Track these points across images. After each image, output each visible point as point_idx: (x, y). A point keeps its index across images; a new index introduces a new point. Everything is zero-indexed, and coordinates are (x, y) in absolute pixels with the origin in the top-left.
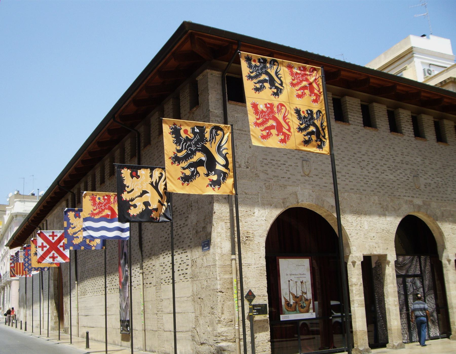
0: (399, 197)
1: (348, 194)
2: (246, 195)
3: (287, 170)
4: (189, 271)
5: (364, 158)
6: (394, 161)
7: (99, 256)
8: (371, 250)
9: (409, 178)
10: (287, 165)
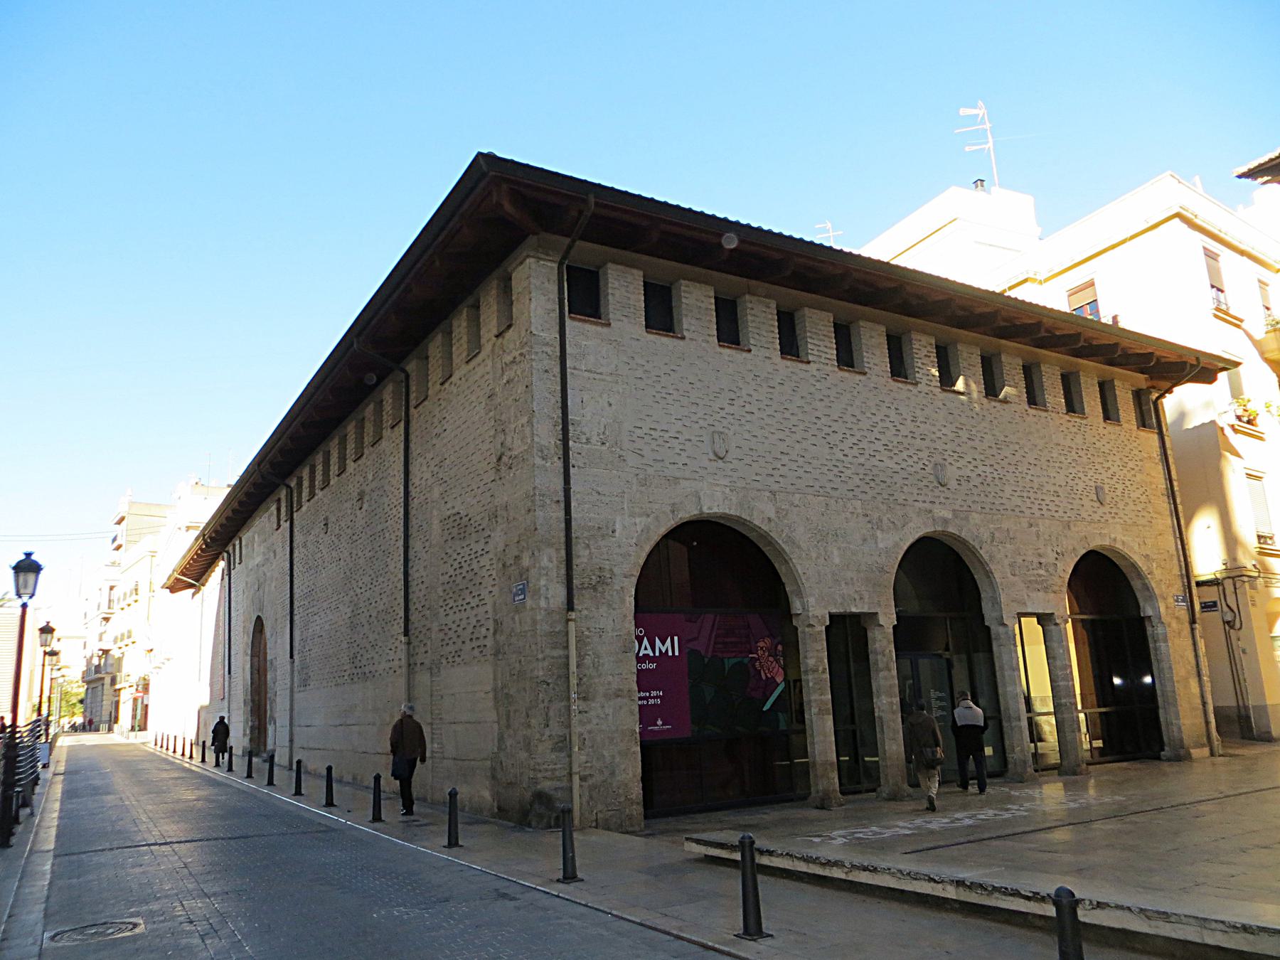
1: (801, 495)
2: (598, 497)
3: (681, 450)
4: (489, 642)
5: (835, 426)
6: (897, 433)
7: (332, 608)
9: (927, 466)
10: (682, 439)
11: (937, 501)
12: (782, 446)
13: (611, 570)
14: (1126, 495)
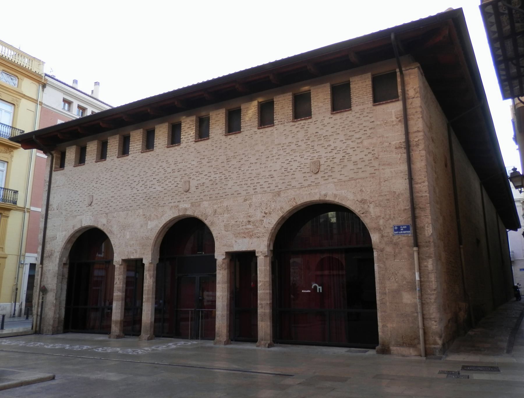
0: (164, 205)
8: (129, 255)
11: (182, 200)
12: (112, 194)
13: (54, 250)
14: (346, 160)
